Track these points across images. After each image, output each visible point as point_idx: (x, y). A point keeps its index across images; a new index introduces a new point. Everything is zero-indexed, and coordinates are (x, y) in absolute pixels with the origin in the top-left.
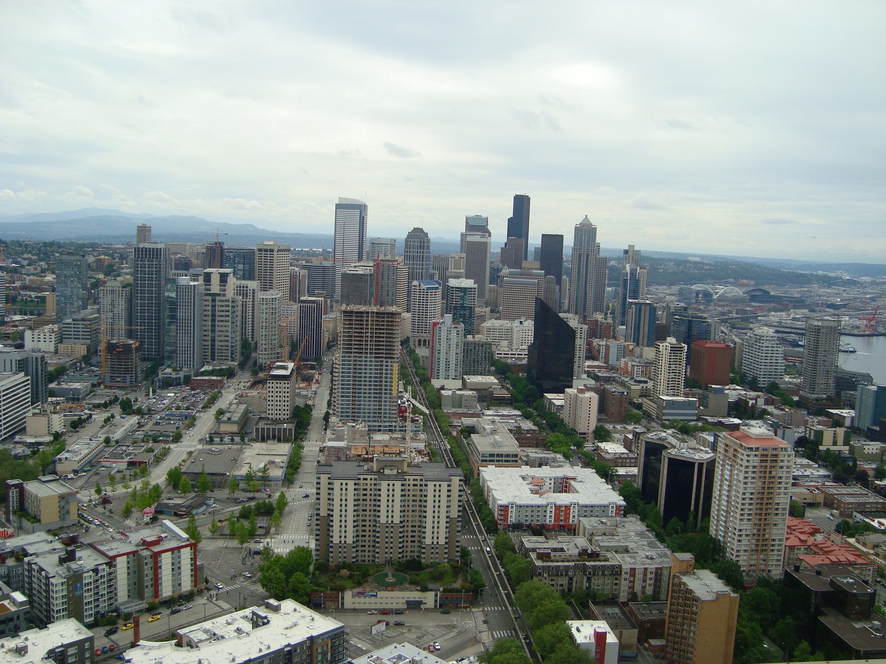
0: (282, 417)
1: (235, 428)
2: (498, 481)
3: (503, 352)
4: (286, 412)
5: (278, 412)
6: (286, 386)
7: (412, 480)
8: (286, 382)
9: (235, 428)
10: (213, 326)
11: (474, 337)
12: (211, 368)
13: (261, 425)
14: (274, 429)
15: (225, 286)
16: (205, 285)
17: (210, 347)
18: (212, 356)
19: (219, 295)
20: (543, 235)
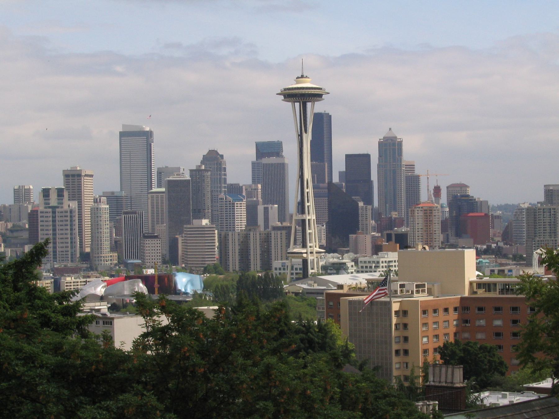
6: (158, 242)
8: (158, 240)
15: (62, 200)
19: (58, 207)
20: (348, 157)
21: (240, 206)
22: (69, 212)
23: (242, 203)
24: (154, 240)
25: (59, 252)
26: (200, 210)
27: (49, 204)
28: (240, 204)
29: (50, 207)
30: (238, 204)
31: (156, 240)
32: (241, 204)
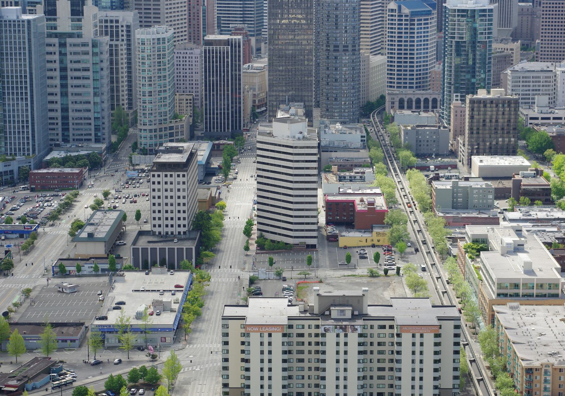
0: (176, 230)
1: (99, 249)
2: (525, 328)
3: (540, 116)
4: (182, 222)
5: (170, 222)
6: (181, 179)
7: (376, 327)
8: (181, 174)
9: (99, 249)
10: (64, 86)
11: (489, 93)
12: (63, 154)
13: (143, 243)
14: (162, 250)
15: (80, 20)
16: (48, 20)
17: (59, 121)
18: (63, 135)
19: (71, 35)
21: (425, 24)
22: (90, 45)
23: (429, 17)
24: (171, 176)
25: (73, 119)
26: (338, 46)
27: (55, 28)
28: (425, 20)
29: (56, 35)
30: (421, 20)
31: (175, 174)
32: (427, 19)
